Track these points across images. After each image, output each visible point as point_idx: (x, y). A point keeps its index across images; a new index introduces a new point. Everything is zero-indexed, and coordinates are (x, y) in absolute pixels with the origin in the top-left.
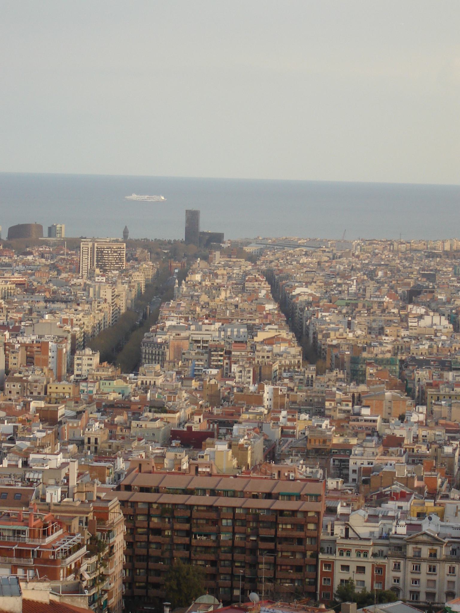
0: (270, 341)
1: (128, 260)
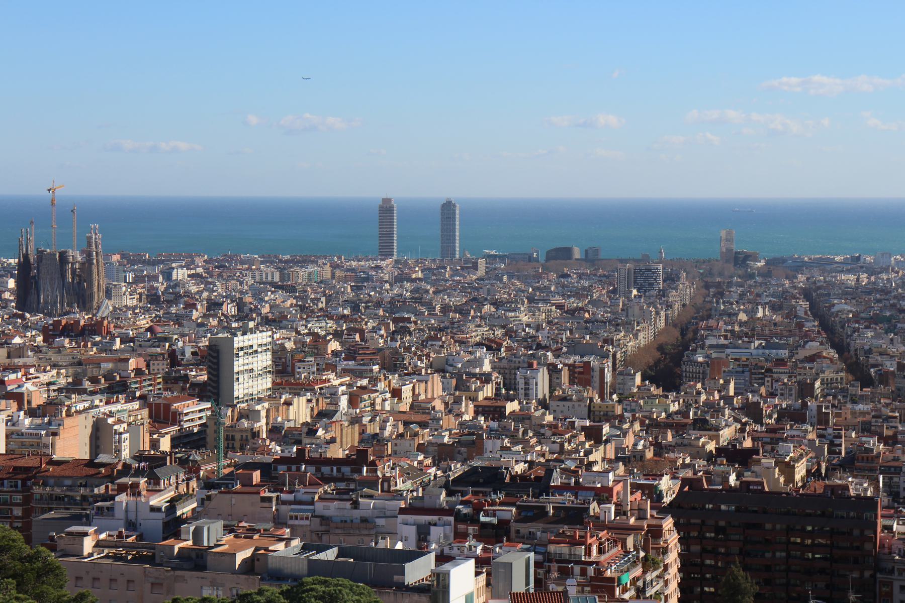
0: (811, 359)
1: (664, 281)
